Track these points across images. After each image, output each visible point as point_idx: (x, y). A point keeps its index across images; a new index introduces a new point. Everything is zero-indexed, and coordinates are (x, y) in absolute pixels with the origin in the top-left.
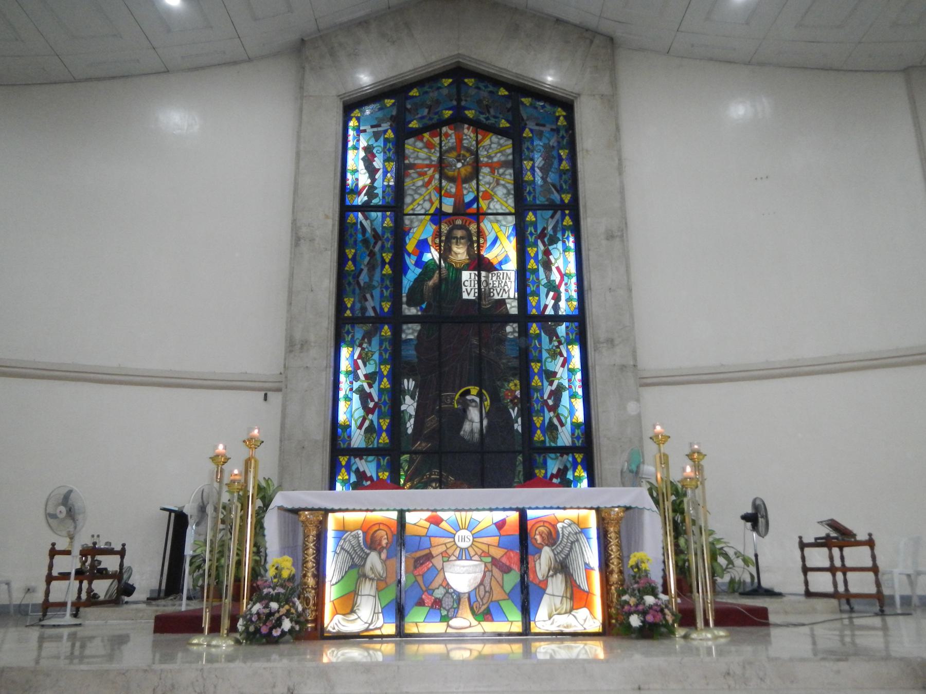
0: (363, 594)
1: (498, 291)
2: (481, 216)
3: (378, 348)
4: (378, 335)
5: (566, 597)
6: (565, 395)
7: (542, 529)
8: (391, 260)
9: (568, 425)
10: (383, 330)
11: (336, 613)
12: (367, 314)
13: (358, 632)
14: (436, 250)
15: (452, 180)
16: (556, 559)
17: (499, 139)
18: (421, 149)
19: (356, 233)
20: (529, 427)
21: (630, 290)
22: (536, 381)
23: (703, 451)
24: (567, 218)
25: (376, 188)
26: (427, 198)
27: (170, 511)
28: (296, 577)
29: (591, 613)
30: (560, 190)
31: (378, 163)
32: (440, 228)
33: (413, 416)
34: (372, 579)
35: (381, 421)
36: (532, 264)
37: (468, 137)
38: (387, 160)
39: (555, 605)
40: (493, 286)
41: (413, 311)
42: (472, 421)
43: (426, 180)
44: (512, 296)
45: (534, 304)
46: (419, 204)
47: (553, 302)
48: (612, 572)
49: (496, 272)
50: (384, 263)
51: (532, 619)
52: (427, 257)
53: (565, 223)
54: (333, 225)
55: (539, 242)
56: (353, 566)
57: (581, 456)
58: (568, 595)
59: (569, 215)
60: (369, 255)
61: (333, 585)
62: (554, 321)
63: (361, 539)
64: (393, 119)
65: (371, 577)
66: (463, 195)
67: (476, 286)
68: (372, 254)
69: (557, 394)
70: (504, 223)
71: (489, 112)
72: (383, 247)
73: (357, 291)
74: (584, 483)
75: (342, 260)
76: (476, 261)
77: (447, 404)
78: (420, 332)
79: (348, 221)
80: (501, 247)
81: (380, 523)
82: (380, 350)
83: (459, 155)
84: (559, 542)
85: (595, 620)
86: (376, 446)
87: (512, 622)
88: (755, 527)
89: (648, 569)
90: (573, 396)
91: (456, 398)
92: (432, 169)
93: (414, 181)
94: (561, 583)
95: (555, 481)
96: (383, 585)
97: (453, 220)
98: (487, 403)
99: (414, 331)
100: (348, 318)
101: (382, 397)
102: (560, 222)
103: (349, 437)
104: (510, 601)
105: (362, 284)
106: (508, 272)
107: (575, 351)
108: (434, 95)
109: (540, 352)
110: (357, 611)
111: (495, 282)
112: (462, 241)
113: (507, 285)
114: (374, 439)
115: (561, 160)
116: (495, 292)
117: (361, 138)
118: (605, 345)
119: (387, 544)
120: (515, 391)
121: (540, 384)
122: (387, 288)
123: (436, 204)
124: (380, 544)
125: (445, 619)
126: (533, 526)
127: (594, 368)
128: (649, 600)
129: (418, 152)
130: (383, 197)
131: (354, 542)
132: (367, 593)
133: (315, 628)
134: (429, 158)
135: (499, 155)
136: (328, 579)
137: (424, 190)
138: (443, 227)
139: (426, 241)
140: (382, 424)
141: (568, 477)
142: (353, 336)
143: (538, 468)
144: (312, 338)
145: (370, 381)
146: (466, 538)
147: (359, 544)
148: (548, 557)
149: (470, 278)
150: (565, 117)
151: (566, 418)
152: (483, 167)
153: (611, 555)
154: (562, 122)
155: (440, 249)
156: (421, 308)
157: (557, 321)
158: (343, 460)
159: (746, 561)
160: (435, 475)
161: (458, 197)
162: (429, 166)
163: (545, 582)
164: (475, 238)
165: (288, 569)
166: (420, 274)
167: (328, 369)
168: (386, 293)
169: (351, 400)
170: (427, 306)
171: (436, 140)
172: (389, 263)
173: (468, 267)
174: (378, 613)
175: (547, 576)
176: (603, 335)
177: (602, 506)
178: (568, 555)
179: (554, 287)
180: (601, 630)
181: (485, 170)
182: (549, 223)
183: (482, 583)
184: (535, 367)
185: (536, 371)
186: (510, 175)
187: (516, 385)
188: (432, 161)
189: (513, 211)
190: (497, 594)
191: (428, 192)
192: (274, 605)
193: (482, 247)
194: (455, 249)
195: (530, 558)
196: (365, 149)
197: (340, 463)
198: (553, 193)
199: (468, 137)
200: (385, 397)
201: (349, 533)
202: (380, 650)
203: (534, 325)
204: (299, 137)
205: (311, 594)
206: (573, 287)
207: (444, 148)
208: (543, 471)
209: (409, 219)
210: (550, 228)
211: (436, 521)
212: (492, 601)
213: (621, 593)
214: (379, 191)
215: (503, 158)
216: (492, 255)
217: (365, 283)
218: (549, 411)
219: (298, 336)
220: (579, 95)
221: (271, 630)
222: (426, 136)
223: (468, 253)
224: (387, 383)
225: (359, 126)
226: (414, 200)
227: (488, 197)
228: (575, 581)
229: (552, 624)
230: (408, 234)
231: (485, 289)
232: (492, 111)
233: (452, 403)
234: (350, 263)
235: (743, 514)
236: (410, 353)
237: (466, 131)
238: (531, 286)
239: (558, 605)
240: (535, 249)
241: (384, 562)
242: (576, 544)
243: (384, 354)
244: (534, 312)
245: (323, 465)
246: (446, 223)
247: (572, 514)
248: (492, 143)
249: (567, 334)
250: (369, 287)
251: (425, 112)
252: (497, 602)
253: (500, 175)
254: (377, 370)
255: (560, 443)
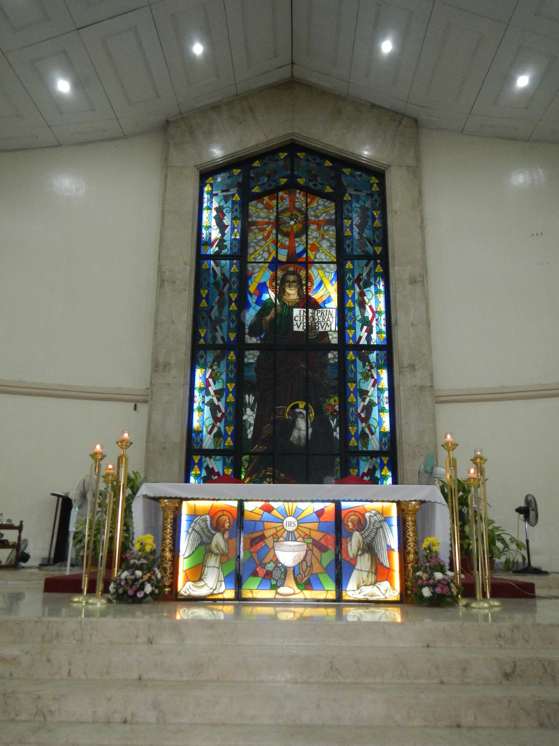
0: (209, 566)
1: (323, 324)
2: (309, 265)
3: (225, 369)
4: (225, 359)
5: (372, 572)
6: (375, 409)
7: (353, 517)
8: (236, 299)
9: (377, 434)
10: (230, 355)
11: (187, 580)
12: (217, 342)
13: (205, 596)
14: (273, 291)
15: (286, 234)
16: (364, 541)
17: (325, 202)
18: (261, 209)
19: (208, 277)
20: (345, 434)
21: (429, 326)
22: (352, 398)
23: (485, 456)
24: (379, 266)
25: (225, 241)
26: (266, 249)
27: (59, 496)
28: (157, 551)
29: (392, 585)
30: (373, 244)
31: (227, 221)
32: (276, 273)
33: (252, 425)
34: (216, 554)
35: (227, 428)
36: (349, 304)
37: (300, 200)
38: (234, 218)
39: (362, 578)
40: (318, 321)
41: (254, 340)
42: (300, 430)
43: (266, 234)
44: (333, 329)
45: (351, 336)
46: (259, 254)
47: (366, 334)
48: (409, 553)
49: (320, 310)
50: (231, 301)
51: (344, 589)
52: (265, 297)
53: (376, 271)
54: (191, 271)
55: (356, 285)
56: (201, 544)
57: (387, 459)
58: (373, 571)
59: (380, 264)
60: (219, 295)
61: (186, 558)
62: (368, 350)
63: (209, 522)
64: (239, 185)
65: (216, 552)
66: (295, 247)
67: (305, 321)
68: (221, 294)
69: (368, 409)
70: (327, 270)
71: (317, 180)
72: (230, 289)
73: (209, 324)
74: (390, 481)
75: (197, 298)
76: (305, 300)
77: (279, 415)
78: (259, 357)
79: (203, 267)
80: (325, 289)
81: (225, 510)
82: (227, 371)
83: (292, 215)
84: (367, 528)
85: (394, 591)
86: (222, 448)
87: (328, 591)
88: (527, 518)
89: (437, 550)
90: (381, 410)
91: (287, 410)
92: (270, 226)
93: (256, 235)
94: (368, 560)
95: (365, 478)
96: (225, 559)
97: (286, 268)
98: (312, 415)
99: (254, 356)
100: (202, 345)
101: (228, 409)
102: (373, 269)
103: (201, 440)
104: (326, 575)
105: (213, 319)
106: (331, 310)
107: (384, 374)
108: (272, 165)
109: (356, 374)
110: (204, 579)
111: (319, 318)
112: (294, 284)
113: (329, 320)
114: (221, 442)
115: (374, 219)
116: (320, 326)
117: (214, 200)
118: (408, 369)
119: (229, 526)
120: (335, 406)
121: (355, 400)
122: (233, 321)
123: (273, 254)
124: (223, 526)
125: (274, 587)
126: (346, 514)
127: (399, 387)
128: (438, 576)
129: (259, 212)
130: (231, 248)
131: (203, 524)
132: (213, 565)
133: (170, 592)
134: (268, 217)
135: (324, 215)
136: (182, 552)
137: (263, 242)
138: (278, 273)
139: (265, 283)
140: (228, 430)
141: (376, 475)
142: (205, 360)
143: (352, 468)
144: (173, 361)
145: (218, 396)
146: (292, 523)
147: (207, 526)
148: (357, 540)
149: (300, 314)
150: (377, 183)
151: (376, 428)
152: (311, 225)
153: (408, 539)
154: (375, 188)
155: (276, 291)
156: (260, 338)
157: (370, 350)
158: (196, 459)
159: (519, 545)
160: (269, 472)
161: (291, 249)
162: (267, 223)
163: (355, 559)
164: (304, 282)
165: (150, 544)
166: (260, 310)
167: (185, 386)
168: (232, 326)
169: (203, 410)
170: (264, 336)
171: (274, 202)
172: (235, 302)
173: (298, 306)
174: (221, 581)
175: (357, 555)
176: (406, 363)
177: (402, 500)
178: (373, 539)
179: (367, 322)
180: (399, 599)
181: (313, 227)
182: (364, 270)
183: (304, 560)
184: (351, 387)
185: (352, 389)
186: (333, 231)
187: (335, 401)
188: (270, 219)
189: (335, 260)
190: (316, 568)
191: (268, 244)
192: (139, 573)
193: (310, 289)
194: (288, 290)
195: (343, 541)
196: (216, 209)
197: (194, 460)
198: (367, 246)
199: (300, 200)
200: (231, 409)
201: (199, 517)
202: (222, 611)
203: (351, 353)
204: (164, 199)
205: (168, 565)
206: (383, 322)
207: (280, 209)
208: (356, 471)
209: (251, 266)
210: (364, 274)
211: (269, 510)
212: (312, 574)
213: (416, 570)
214: (228, 243)
215: (327, 218)
216: (317, 296)
217: (215, 317)
218: (362, 422)
219: (162, 358)
220: (389, 166)
221: (136, 592)
222: (266, 199)
223: (299, 294)
224: (233, 398)
225: (212, 191)
226: (256, 251)
227: (315, 248)
228: (379, 559)
229: (360, 593)
230: (250, 278)
231: (312, 323)
232: (319, 179)
233: (284, 414)
234: (204, 301)
235: (517, 507)
236: (251, 374)
237: (298, 195)
238: (349, 321)
239: (365, 578)
240: (353, 291)
241: (226, 541)
242: (381, 530)
243: (230, 374)
244: (351, 342)
245: (180, 463)
246: (281, 270)
247: (378, 505)
248: (319, 205)
249: (377, 360)
250: (219, 321)
251: (265, 179)
252: (316, 574)
253: (325, 231)
254: (225, 387)
255: (370, 448)
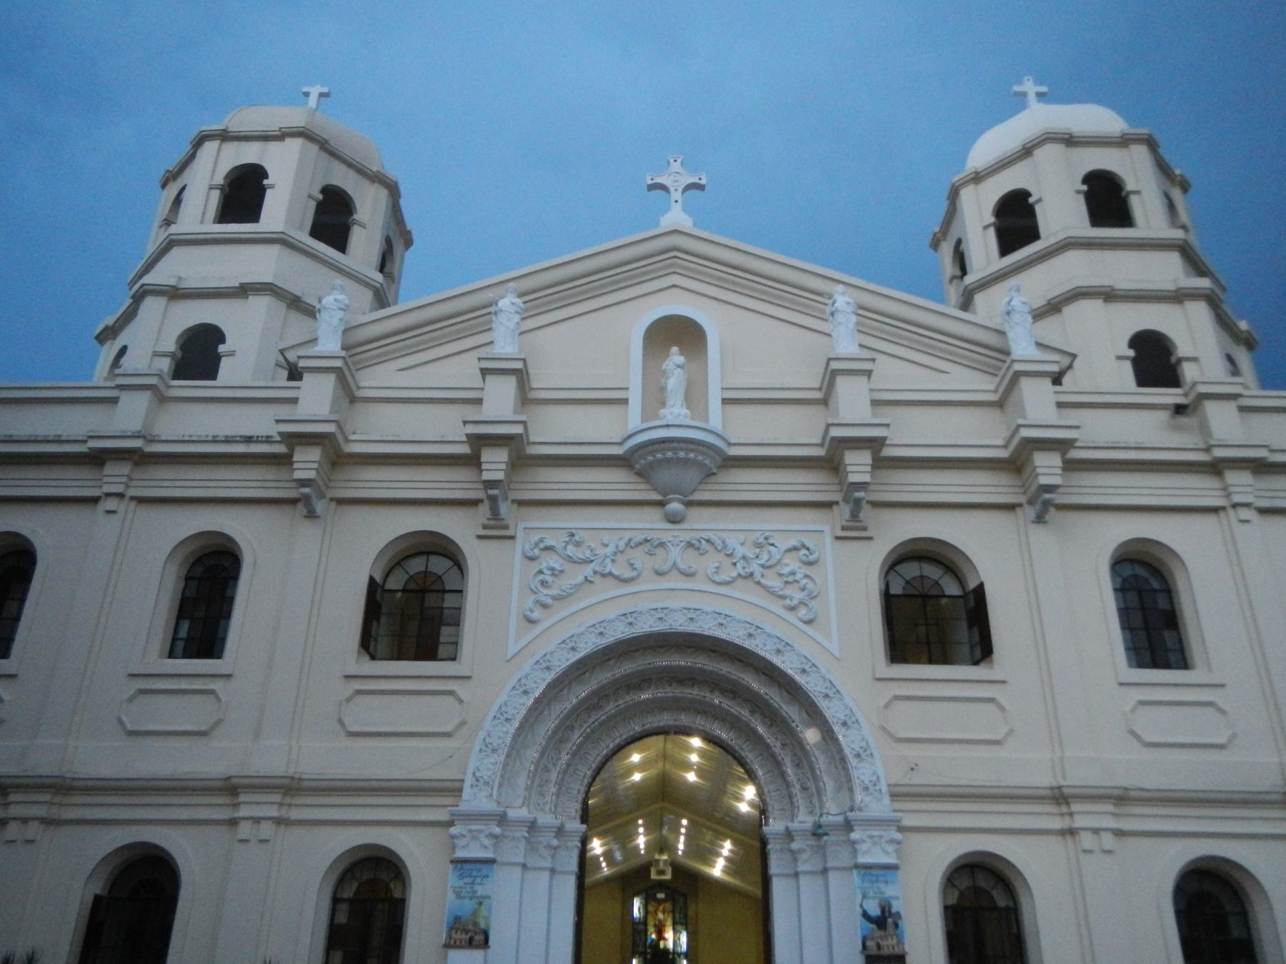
41: (649, 951)
